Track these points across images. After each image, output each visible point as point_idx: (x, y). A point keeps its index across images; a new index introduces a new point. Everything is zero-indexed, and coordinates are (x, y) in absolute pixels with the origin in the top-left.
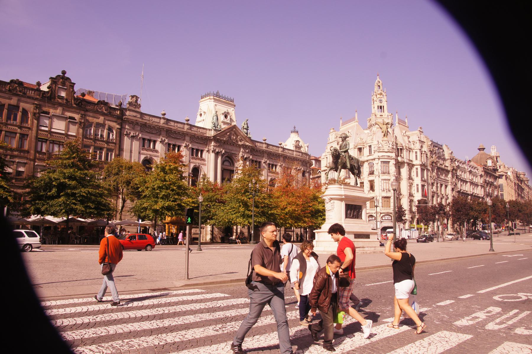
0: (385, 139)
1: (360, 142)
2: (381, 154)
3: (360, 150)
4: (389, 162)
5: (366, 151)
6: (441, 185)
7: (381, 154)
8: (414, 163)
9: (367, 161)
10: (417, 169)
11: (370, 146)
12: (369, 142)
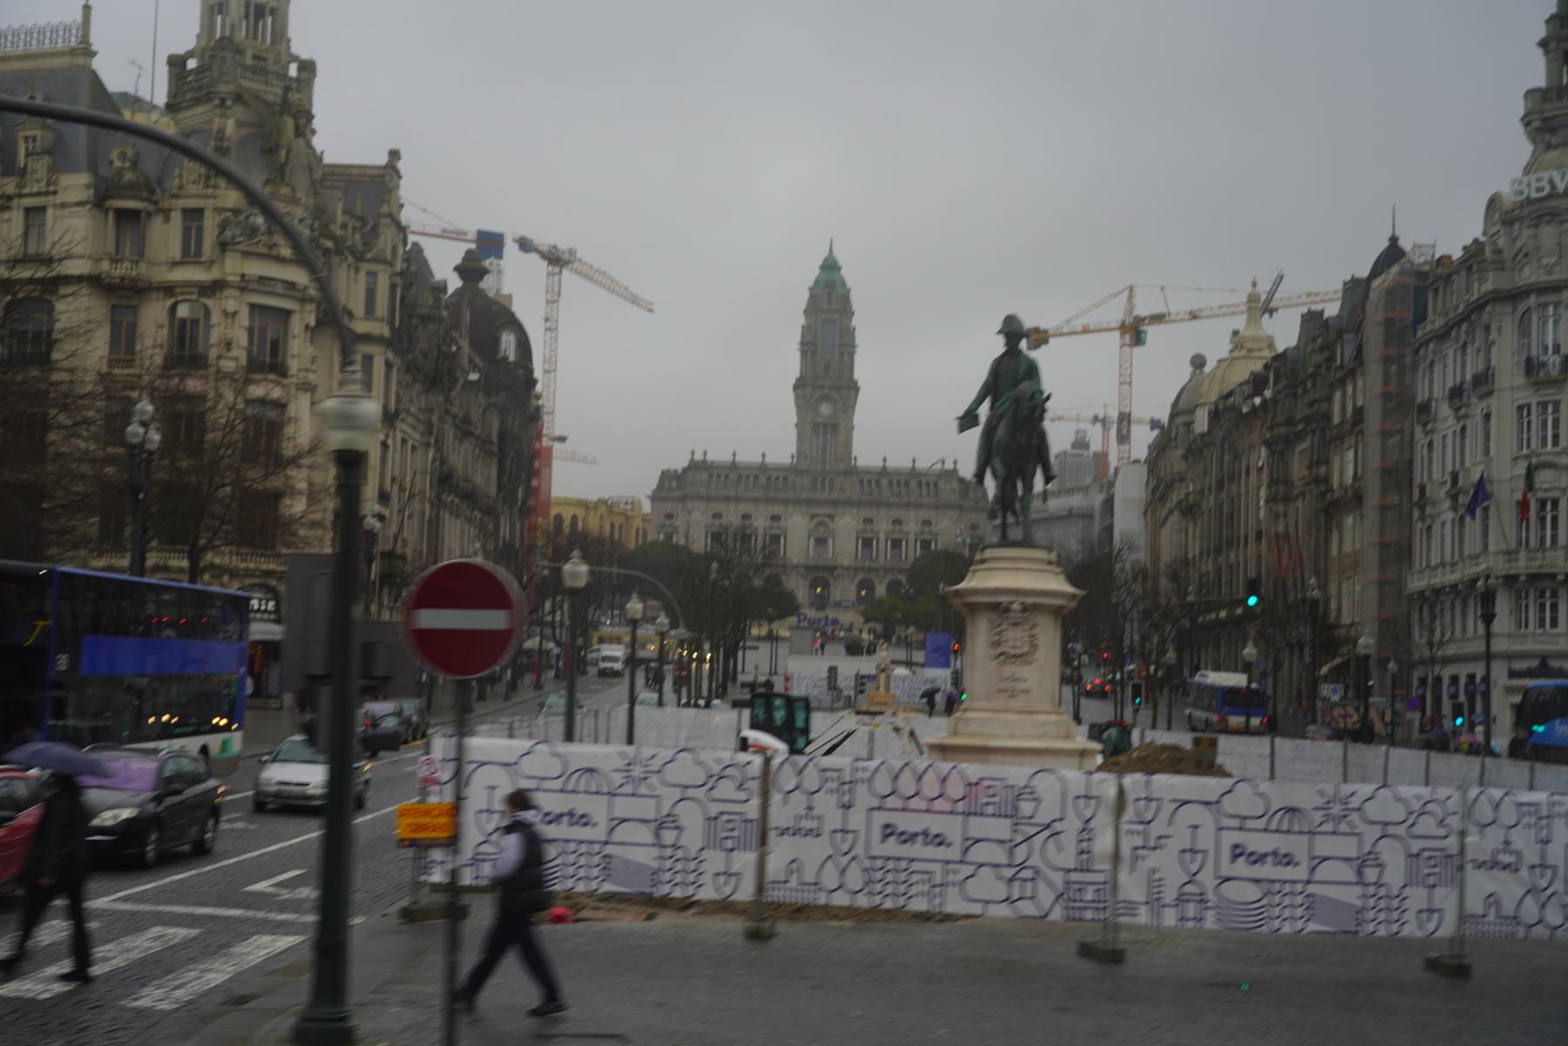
0: (284, 190)
1: (128, 176)
2: (256, 268)
3: (126, 217)
4: (288, 314)
5: (165, 237)
6: (404, 441)
7: (256, 268)
8: (360, 327)
9: (169, 289)
10: (368, 360)
11: (193, 216)
12: (192, 189)
